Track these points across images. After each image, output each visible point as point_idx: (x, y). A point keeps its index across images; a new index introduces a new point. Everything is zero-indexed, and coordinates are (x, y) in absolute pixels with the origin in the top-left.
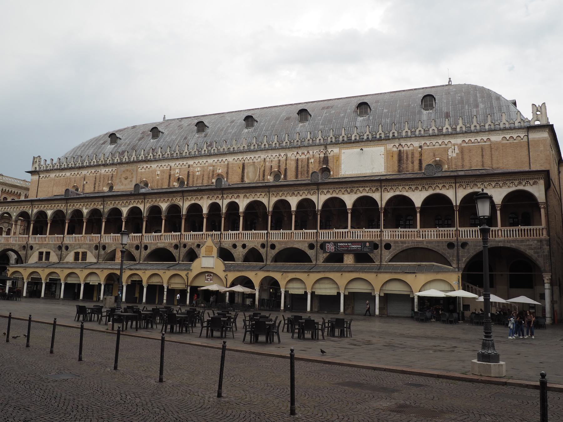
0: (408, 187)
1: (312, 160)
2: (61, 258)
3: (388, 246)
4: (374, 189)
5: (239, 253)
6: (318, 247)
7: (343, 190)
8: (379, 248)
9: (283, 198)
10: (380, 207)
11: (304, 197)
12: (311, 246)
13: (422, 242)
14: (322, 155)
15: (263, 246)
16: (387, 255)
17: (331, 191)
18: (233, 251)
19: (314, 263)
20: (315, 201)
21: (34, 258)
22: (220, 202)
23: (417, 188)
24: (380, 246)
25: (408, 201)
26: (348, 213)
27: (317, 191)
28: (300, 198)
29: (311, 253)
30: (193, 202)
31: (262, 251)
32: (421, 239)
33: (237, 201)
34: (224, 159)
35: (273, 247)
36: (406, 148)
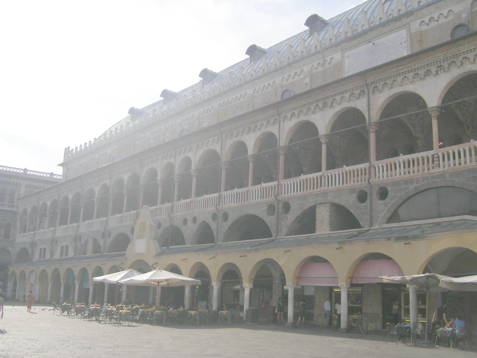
0: (412, 74)
1: (307, 80)
2: (52, 254)
3: (383, 194)
4: (357, 92)
5: (189, 231)
6: (280, 210)
7: (312, 107)
8: (369, 198)
9: (238, 138)
10: (367, 122)
11: (263, 130)
12: (271, 209)
13: (442, 176)
14: (320, 69)
15: (214, 217)
16: (382, 209)
17: (296, 112)
18: (183, 229)
19: (274, 235)
20: (276, 133)
21: (36, 258)
22: (172, 160)
23: (428, 73)
24: (369, 194)
25: (416, 100)
26: (320, 144)
27: (277, 117)
28: (259, 133)
29: (270, 220)
30: (150, 166)
31: (213, 225)
32: (441, 169)
33: (190, 155)
34: (210, 107)
35: (226, 216)
36: (442, 20)
